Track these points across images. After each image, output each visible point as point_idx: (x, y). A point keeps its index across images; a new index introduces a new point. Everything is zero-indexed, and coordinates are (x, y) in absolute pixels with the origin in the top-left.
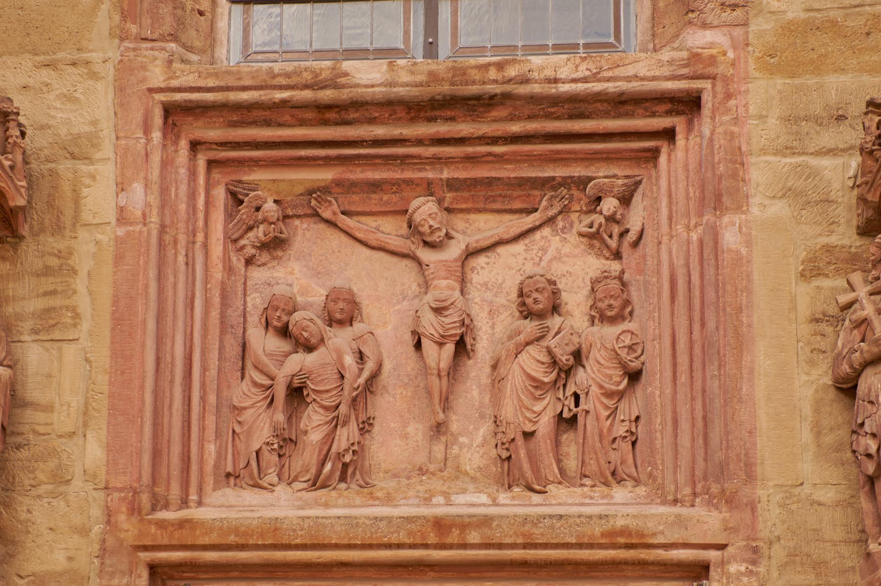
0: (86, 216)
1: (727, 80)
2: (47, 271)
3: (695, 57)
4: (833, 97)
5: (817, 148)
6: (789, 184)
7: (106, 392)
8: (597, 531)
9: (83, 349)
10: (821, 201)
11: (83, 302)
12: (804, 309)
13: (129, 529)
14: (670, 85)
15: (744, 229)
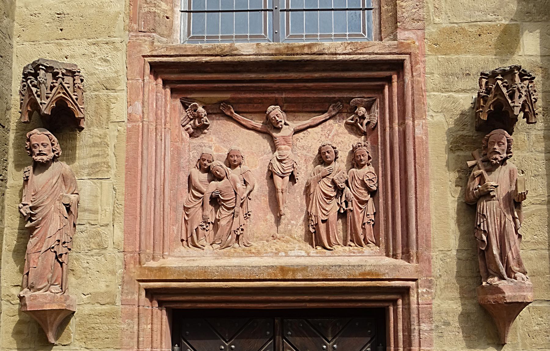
7: (123, 204)
9: (112, 183)
11: (112, 160)
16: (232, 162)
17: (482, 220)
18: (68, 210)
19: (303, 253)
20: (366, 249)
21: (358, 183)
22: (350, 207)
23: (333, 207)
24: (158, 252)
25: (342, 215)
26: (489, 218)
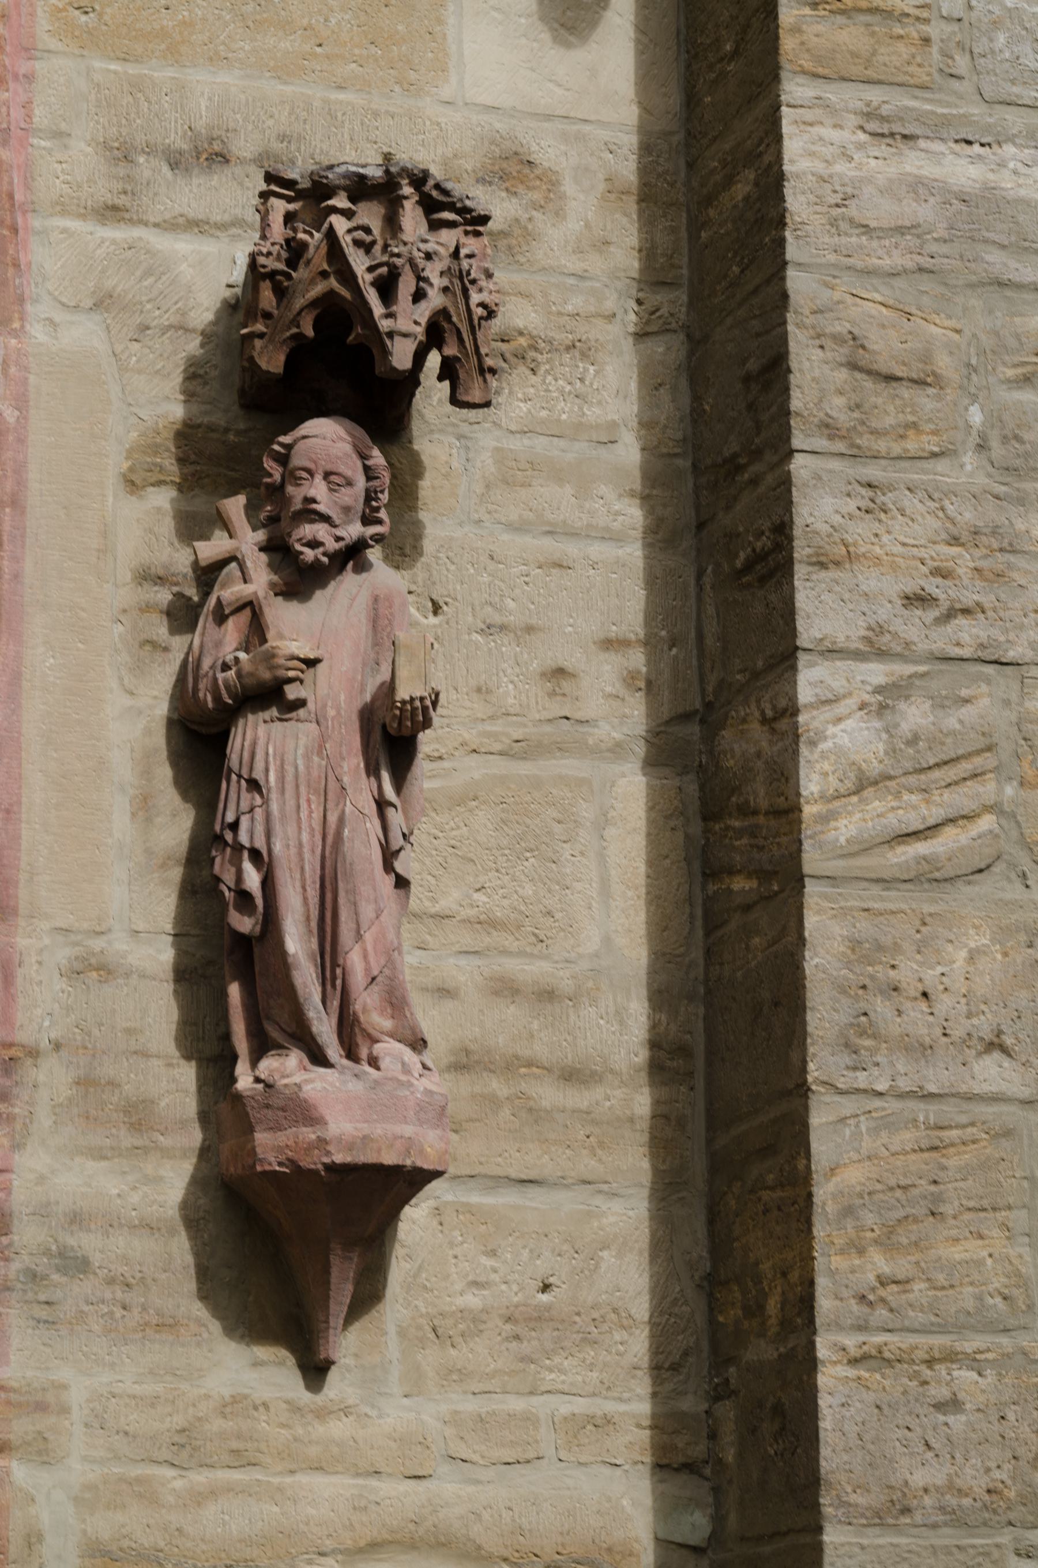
5: (167, 216)
6: (109, 284)
10: (171, 327)
15: (13, 370)
17: (244, 806)
26: (274, 796)
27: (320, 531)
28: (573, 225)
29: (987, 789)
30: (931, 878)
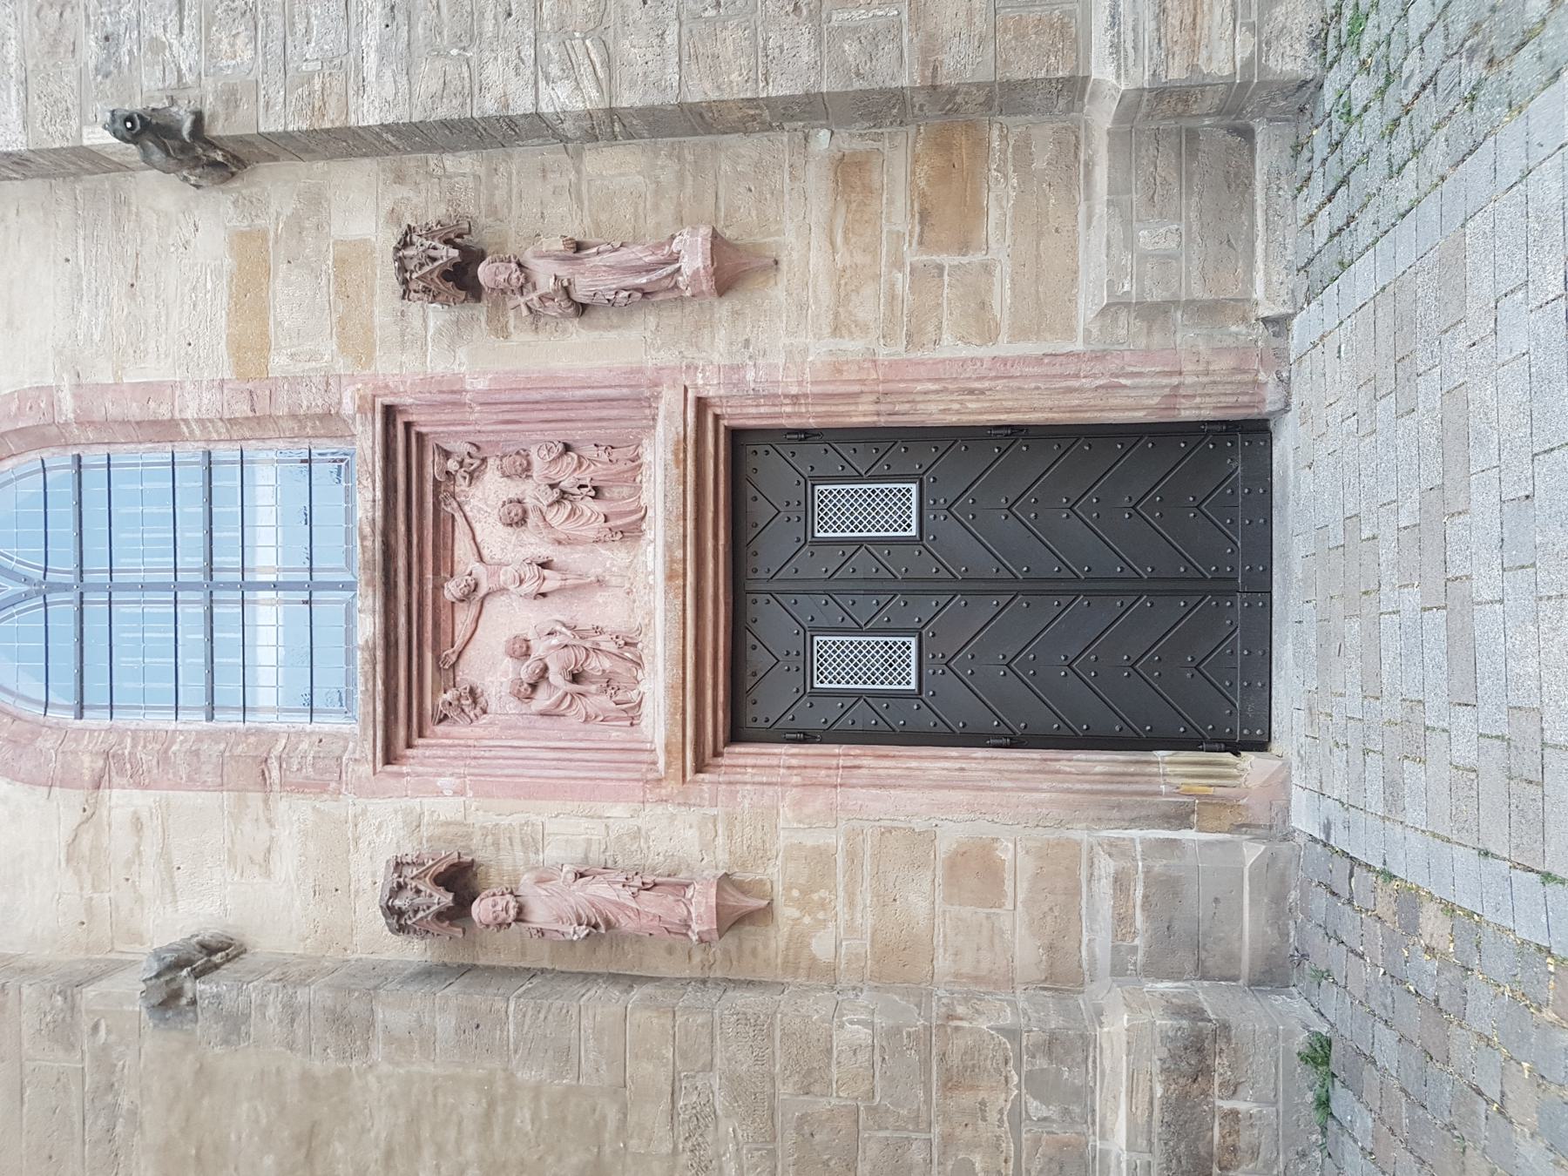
0: (459, 817)
1: (376, 387)
2: (496, 844)
3: (360, 409)
4: (389, 319)
8: (675, 471)
11: (517, 819)
12: (529, 337)
13: (671, 787)
14: (379, 425)
16: (522, 650)
18: (582, 876)
19: (650, 548)
20: (647, 457)
21: (553, 472)
22: (587, 482)
23: (588, 506)
24: (645, 757)
25: (597, 493)
27: (514, 276)
28: (411, 194)
29: (577, 43)
30: (608, 63)
